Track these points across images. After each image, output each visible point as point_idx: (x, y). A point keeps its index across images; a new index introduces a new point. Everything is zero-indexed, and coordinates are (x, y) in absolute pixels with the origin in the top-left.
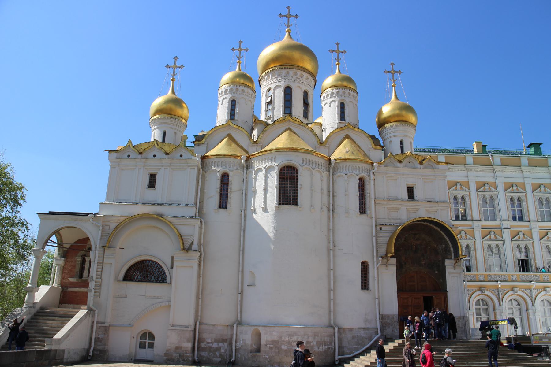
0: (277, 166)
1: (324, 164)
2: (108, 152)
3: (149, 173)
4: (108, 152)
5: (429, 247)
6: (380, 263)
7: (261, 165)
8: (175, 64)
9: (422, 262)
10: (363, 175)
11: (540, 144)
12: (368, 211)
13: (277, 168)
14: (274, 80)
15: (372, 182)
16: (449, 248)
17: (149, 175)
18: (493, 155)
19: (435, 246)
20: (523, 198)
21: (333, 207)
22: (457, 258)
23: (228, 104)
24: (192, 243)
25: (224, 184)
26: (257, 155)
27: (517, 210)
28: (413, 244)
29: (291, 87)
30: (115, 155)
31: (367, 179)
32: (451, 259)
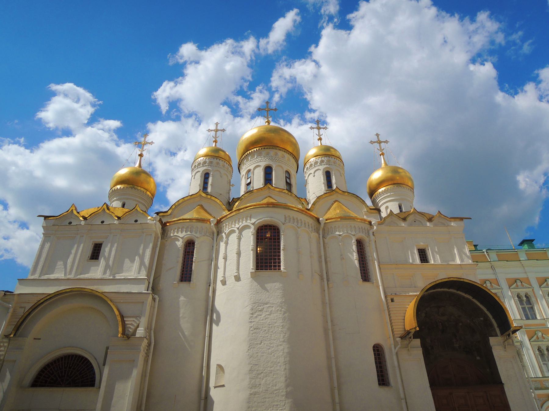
0: (253, 224)
1: (311, 224)
2: (44, 218)
4: (44, 218)
5: (461, 324)
6: (399, 346)
7: (233, 226)
9: (455, 345)
10: (361, 235)
11: (533, 240)
12: (372, 277)
13: (253, 227)
14: (253, 161)
15: (373, 243)
16: (490, 320)
17: (93, 245)
18: (487, 251)
19: (469, 321)
20: (531, 294)
21: (327, 276)
22: (507, 333)
23: (200, 177)
24: (138, 327)
25: (188, 252)
26: (229, 216)
27: (528, 307)
28: (438, 321)
29: (271, 166)
30: (51, 221)
31: (366, 239)
32: (497, 335)
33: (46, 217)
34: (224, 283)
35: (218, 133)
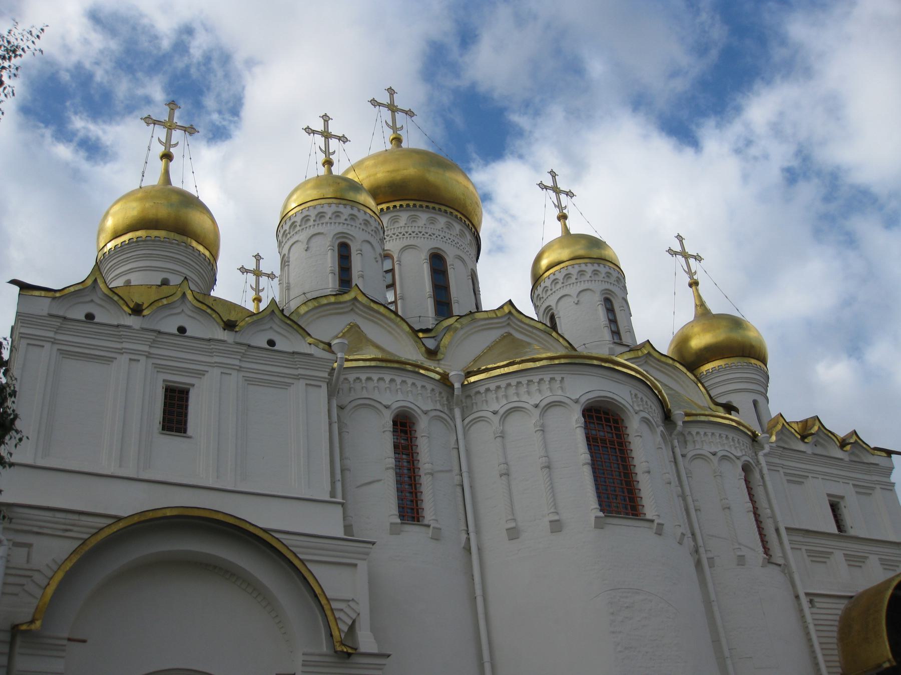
3: (164, 381)
8: (171, 116)
25: (405, 448)
33: (24, 287)
34: (513, 534)
35: (334, 144)
